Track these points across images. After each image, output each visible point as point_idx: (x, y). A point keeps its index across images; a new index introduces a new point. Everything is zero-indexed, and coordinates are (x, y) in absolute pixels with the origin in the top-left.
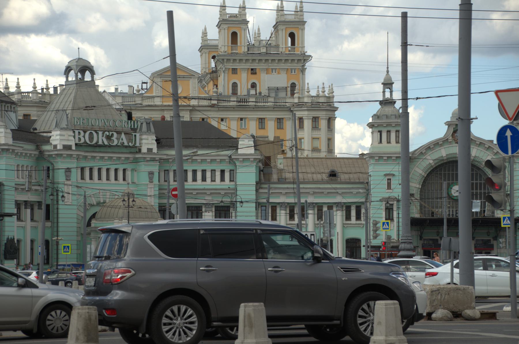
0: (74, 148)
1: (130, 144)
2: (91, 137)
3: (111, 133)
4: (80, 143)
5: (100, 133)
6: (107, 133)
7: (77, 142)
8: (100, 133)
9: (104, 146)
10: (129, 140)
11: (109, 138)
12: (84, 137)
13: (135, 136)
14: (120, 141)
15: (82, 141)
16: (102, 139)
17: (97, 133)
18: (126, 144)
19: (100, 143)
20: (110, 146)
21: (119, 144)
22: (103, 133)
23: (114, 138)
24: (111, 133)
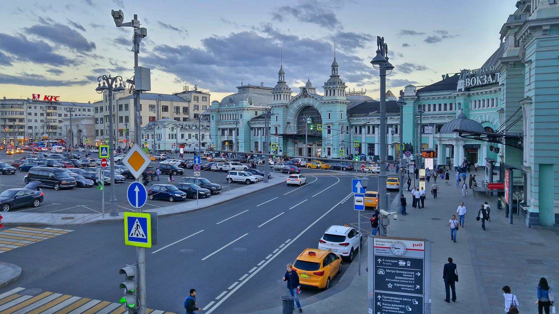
0: (463, 90)
1: (494, 81)
2: (473, 83)
3: (483, 76)
4: (468, 86)
5: (478, 78)
6: (481, 77)
7: (467, 86)
8: (478, 78)
9: (479, 86)
10: (493, 78)
11: (482, 81)
12: (470, 82)
13: (497, 74)
14: (488, 80)
15: (469, 85)
16: (479, 82)
17: (477, 79)
18: (491, 82)
19: (478, 84)
20: (483, 86)
21: (488, 83)
22: (479, 78)
23: (485, 80)
24: (483, 76)
